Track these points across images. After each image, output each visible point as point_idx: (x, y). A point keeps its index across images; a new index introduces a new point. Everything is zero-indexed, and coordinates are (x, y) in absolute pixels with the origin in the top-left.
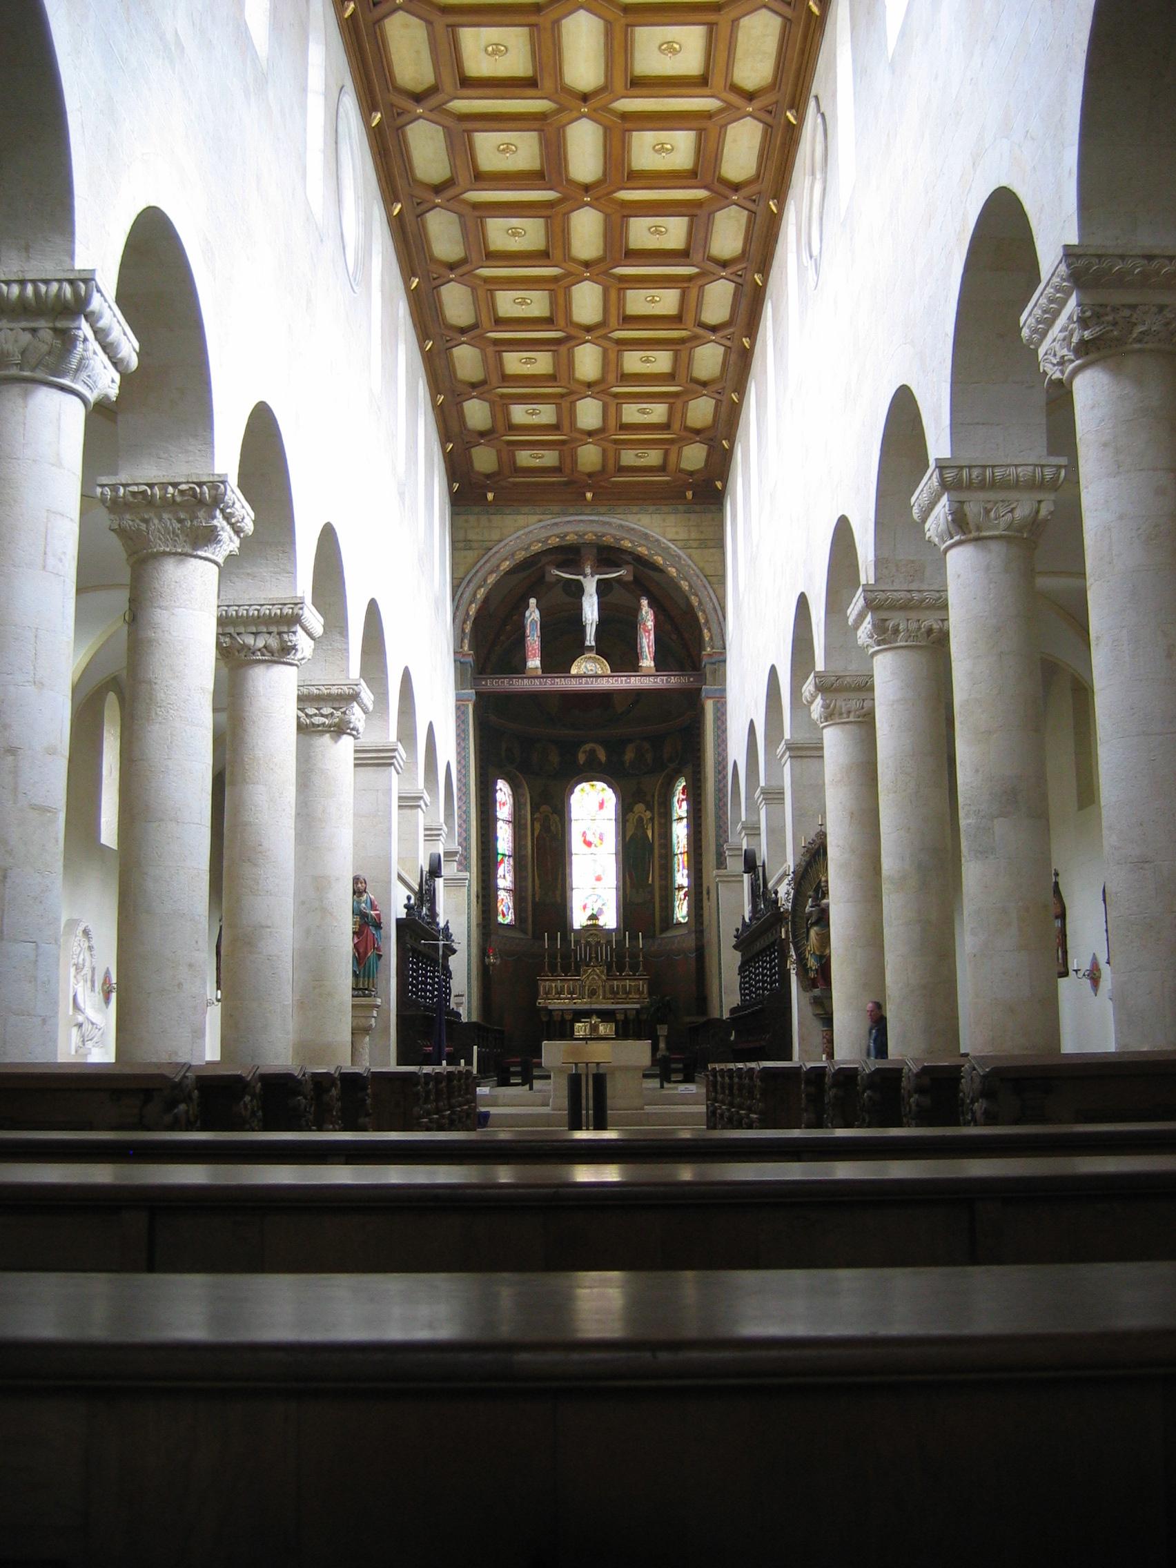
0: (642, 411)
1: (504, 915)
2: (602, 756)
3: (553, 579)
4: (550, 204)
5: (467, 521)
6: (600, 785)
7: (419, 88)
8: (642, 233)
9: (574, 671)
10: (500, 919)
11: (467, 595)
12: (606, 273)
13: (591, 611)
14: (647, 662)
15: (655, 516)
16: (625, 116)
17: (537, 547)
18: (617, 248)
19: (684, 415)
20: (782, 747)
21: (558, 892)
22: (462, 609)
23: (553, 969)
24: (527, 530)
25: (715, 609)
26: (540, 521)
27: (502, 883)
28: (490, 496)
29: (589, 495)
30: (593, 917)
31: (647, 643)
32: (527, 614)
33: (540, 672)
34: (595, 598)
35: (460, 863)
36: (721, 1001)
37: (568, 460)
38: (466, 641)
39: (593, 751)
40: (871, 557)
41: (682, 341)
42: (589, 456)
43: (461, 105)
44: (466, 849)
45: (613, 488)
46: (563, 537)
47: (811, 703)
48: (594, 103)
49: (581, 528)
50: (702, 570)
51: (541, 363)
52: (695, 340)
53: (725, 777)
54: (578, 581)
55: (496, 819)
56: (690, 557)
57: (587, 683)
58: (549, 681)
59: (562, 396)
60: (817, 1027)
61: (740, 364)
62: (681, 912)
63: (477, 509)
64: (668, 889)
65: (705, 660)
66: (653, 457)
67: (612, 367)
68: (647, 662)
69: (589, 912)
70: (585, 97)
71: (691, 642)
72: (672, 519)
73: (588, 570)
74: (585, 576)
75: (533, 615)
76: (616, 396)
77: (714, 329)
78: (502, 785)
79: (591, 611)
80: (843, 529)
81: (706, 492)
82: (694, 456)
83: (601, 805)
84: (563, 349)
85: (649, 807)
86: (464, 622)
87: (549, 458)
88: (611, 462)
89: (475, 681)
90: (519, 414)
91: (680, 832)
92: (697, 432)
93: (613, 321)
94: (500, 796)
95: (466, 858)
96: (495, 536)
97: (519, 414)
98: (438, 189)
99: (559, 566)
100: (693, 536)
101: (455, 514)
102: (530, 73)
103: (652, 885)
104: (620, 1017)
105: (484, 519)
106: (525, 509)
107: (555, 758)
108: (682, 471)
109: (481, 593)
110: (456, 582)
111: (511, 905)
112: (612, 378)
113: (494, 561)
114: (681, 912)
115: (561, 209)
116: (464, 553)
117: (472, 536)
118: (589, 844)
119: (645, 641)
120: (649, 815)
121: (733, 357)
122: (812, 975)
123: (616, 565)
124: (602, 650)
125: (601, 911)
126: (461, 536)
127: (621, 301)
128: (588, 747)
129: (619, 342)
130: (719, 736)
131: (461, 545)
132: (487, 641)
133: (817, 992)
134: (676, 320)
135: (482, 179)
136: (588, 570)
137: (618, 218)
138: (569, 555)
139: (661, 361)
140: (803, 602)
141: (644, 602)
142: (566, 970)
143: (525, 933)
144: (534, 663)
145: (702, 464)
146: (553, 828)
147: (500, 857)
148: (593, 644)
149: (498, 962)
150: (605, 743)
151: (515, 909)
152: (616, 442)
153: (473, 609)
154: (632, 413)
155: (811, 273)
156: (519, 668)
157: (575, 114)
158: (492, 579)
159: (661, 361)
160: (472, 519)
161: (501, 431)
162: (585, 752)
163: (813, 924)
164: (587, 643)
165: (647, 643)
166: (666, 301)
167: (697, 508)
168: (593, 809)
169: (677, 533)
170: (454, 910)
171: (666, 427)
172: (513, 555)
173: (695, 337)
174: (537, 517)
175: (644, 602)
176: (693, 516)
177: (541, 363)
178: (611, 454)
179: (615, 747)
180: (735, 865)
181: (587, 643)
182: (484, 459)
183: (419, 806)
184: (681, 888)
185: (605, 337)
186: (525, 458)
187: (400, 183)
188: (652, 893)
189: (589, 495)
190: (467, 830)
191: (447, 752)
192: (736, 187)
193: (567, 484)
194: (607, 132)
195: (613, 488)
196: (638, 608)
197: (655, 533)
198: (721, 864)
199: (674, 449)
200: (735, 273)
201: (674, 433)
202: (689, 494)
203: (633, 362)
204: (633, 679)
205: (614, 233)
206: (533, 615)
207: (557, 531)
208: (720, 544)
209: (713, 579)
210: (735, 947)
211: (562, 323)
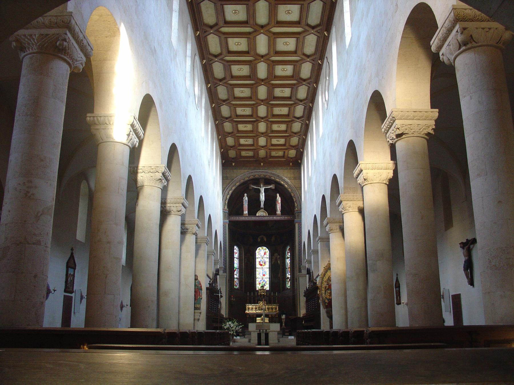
0: (278, 141)
2: (265, 240)
4: (252, 84)
6: (264, 248)
7: (216, 54)
8: (278, 92)
9: (257, 215)
11: (227, 192)
12: (268, 103)
13: (262, 197)
14: (279, 212)
16: (273, 61)
17: (247, 179)
18: (271, 97)
19: (289, 143)
20: (317, 239)
27: (235, 276)
28: (233, 164)
29: (262, 164)
30: (262, 287)
31: (279, 207)
34: (264, 194)
35: (224, 271)
39: (262, 238)
40: (343, 186)
41: (289, 121)
42: (262, 153)
43: (228, 58)
45: (270, 162)
47: (326, 226)
48: (265, 58)
49: (260, 174)
51: (249, 127)
52: (292, 121)
53: (301, 246)
55: (234, 258)
59: (254, 136)
60: (328, 320)
61: (306, 129)
62: (288, 285)
64: (284, 278)
65: (296, 212)
66: (280, 153)
67: (269, 128)
68: (279, 212)
69: (261, 285)
70: (262, 56)
71: (292, 206)
72: (286, 171)
73: (262, 186)
75: (246, 198)
76: (270, 136)
77: (298, 118)
78: (235, 247)
79: (262, 197)
80: (335, 177)
81: (296, 163)
82: (292, 153)
83: (265, 254)
84: (255, 124)
85: (279, 255)
87: (251, 154)
88: (268, 154)
89: (229, 218)
90: (242, 141)
91: (288, 261)
92: (293, 147)
93: (269, 116)
94: (235, 251)
96: (235, 176)
97: (242, 141)
98: (221, 80)
99: (253, 184)
100: (292, 176)
102: (247, 50)
108: (289, 157)
109: (231, 192)
112: (269, 132)
114: (288, 285)
115: (256, 85)
117: (228, 175)
118: (261, 265)
119: (278, 206)
120: (279, 257)
121: (303, 126)
122: (326, 304)
123: (270, 184)
124: (266, 209)
125: (264, 285)
127: (272, 111)
128: (261, 237)
129: (271, 122)
132: (233, 205)
134: (288, 116)
135: (233, 77)
137: (271, 88)
138: (256, 181)
139: (283, 127)
140: (324, 197)
141: (278, 195)
144: (246, 212)
145: (295, 156)
152: (270, 149)
153: (228, 197)
154: (274, 141)
155: (326, 105)
156: (241, 214)
157: (260, 61)
158: (234, 188)
159: (283, 127)
160: (229, 170)
161: (237, 146)
165: (279, 207)
166: (284, 111)
168: (262, 254)
170: (222, 285)
171: (284, 145)
173: (293, 120)
175: (278, 195)
176: (292, 170)
177: (249, 127)
178: (268, 153)
180: (304, 272)
182: (232, 154)
184: (288, 278)
185: (267, 120)
186: (244, 153)
187: (210, 79)
189: (262, 164)
190: (226, 261)
191: (220, 238)
192: (304, 80)
193: (255, 161)
194: (269, 65)
195: (270, 162)
196: (276, 197)
197: (281, 175)
198: (300, 271)
199: (286, 152)
200: (304, 103)
201: (287, 146)
202: (291, 164)
203: (275, 127)
205: (270, 93)
206: (246, 198)
207: (253, 174)
209: (298, 189)
210: (304, 296)
211: (255, 116)
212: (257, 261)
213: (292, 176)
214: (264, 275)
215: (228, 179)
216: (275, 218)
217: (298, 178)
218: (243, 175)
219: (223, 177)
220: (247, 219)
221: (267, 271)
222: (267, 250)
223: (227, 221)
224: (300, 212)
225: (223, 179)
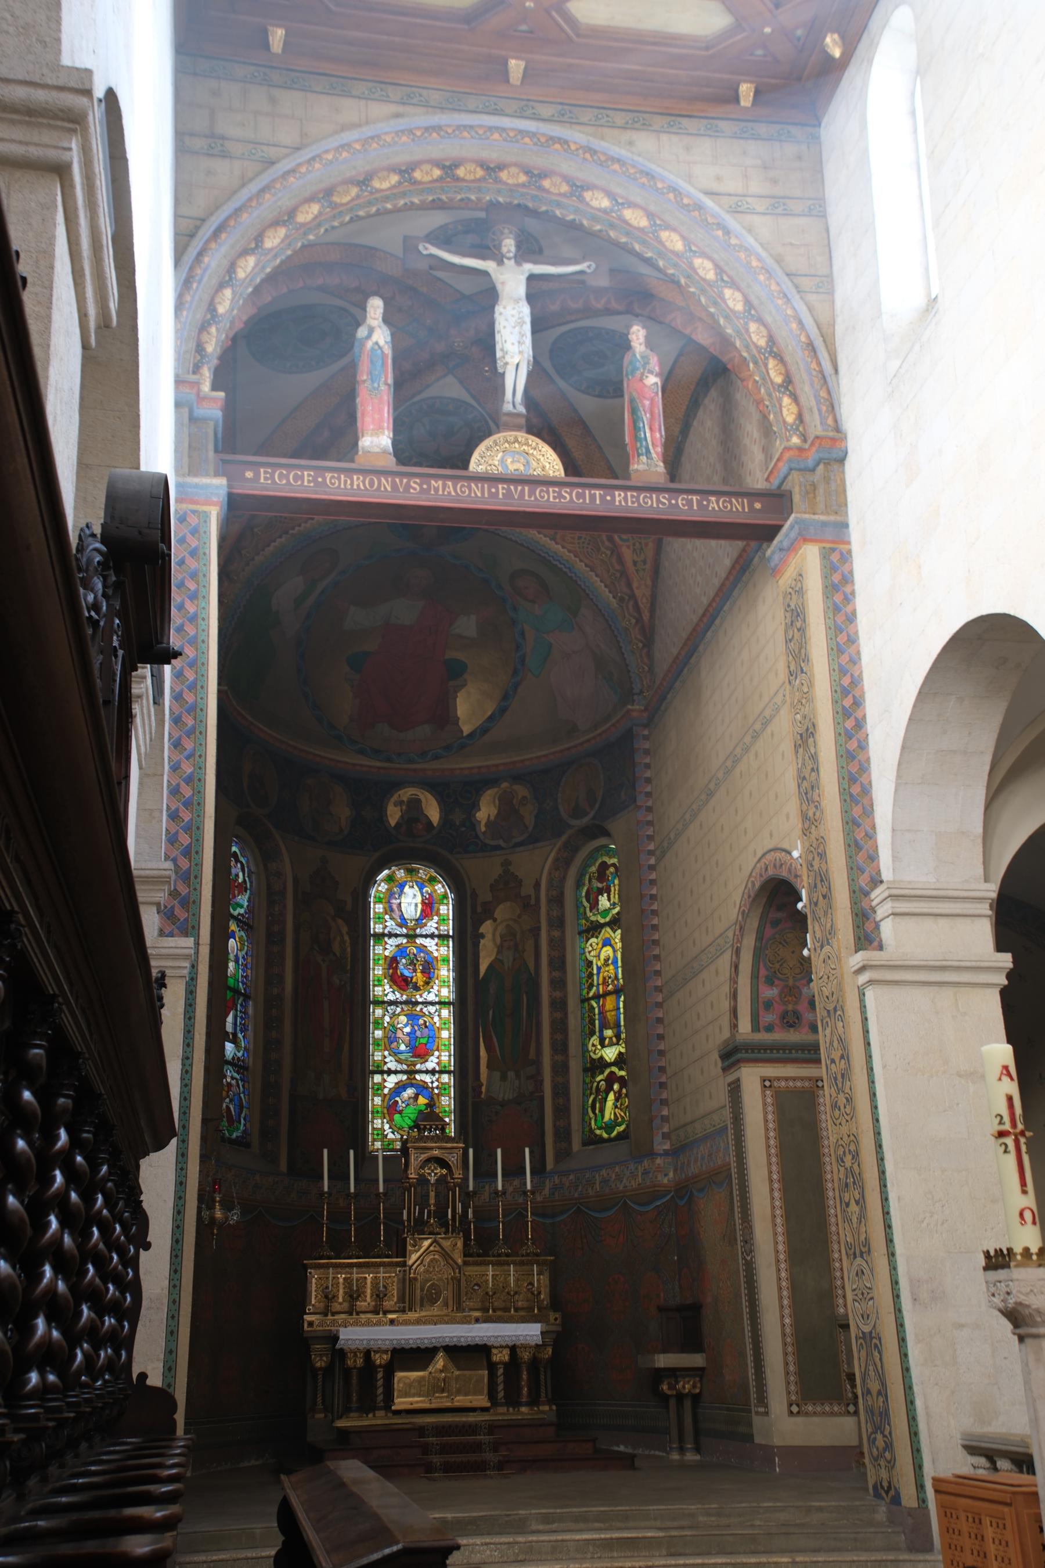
2: (433, 812)
9: (477, 464)
15: (664, 137)
22: (200, 292)
23: (339, 1247)
24: (367, 131)
25: (811, 347)
26: (398, 115)
28: (277, 36)
32: (362, 332)
33: (390, 462)
36: (900, 1325)
38: (207, 375)
39: (415, 804)
44: (189, 877)
46: (449, 168)
50: (779, 260)
54: (486, 274)
56: (750, 231)
57: (508, 494)
58: (415, 485)
72: (705, 146)
83: (429, 907)
86: (203, 328)
95: (189, 903)
103: (538, 1063)
104: (501, 1356)
107: (343, 812)
113: (286, 202)
128: (407, 793)
130: (838, 630)
136: (509, 245)
142: (367, 1247)
144: (377, 440)
147: (229, 994)
148: (522, 409)
149: (235, 1217)
150: (439, 788)
162: (400, 803)
164: (508, 407)
167: (763, 129)
169: (718, 179)
172: (329, 192)
174: (393, 108)
179: (458, 795)
181: (508, 407)
183: (61, 171)
188: (537, 1079)
189: (516, 66)
198: (866, 937)
204: (619, 496)
208: (817, 209)
209: (805, 283)
212: (380, 952)
213: (756, 186)
214: (421, 1052)
215: (225, 155)
216: (622, 502)
217: (806, 200)
221: (443, 1023)
222: (440, 888)
223: (217, 486)
224: (830, 453)
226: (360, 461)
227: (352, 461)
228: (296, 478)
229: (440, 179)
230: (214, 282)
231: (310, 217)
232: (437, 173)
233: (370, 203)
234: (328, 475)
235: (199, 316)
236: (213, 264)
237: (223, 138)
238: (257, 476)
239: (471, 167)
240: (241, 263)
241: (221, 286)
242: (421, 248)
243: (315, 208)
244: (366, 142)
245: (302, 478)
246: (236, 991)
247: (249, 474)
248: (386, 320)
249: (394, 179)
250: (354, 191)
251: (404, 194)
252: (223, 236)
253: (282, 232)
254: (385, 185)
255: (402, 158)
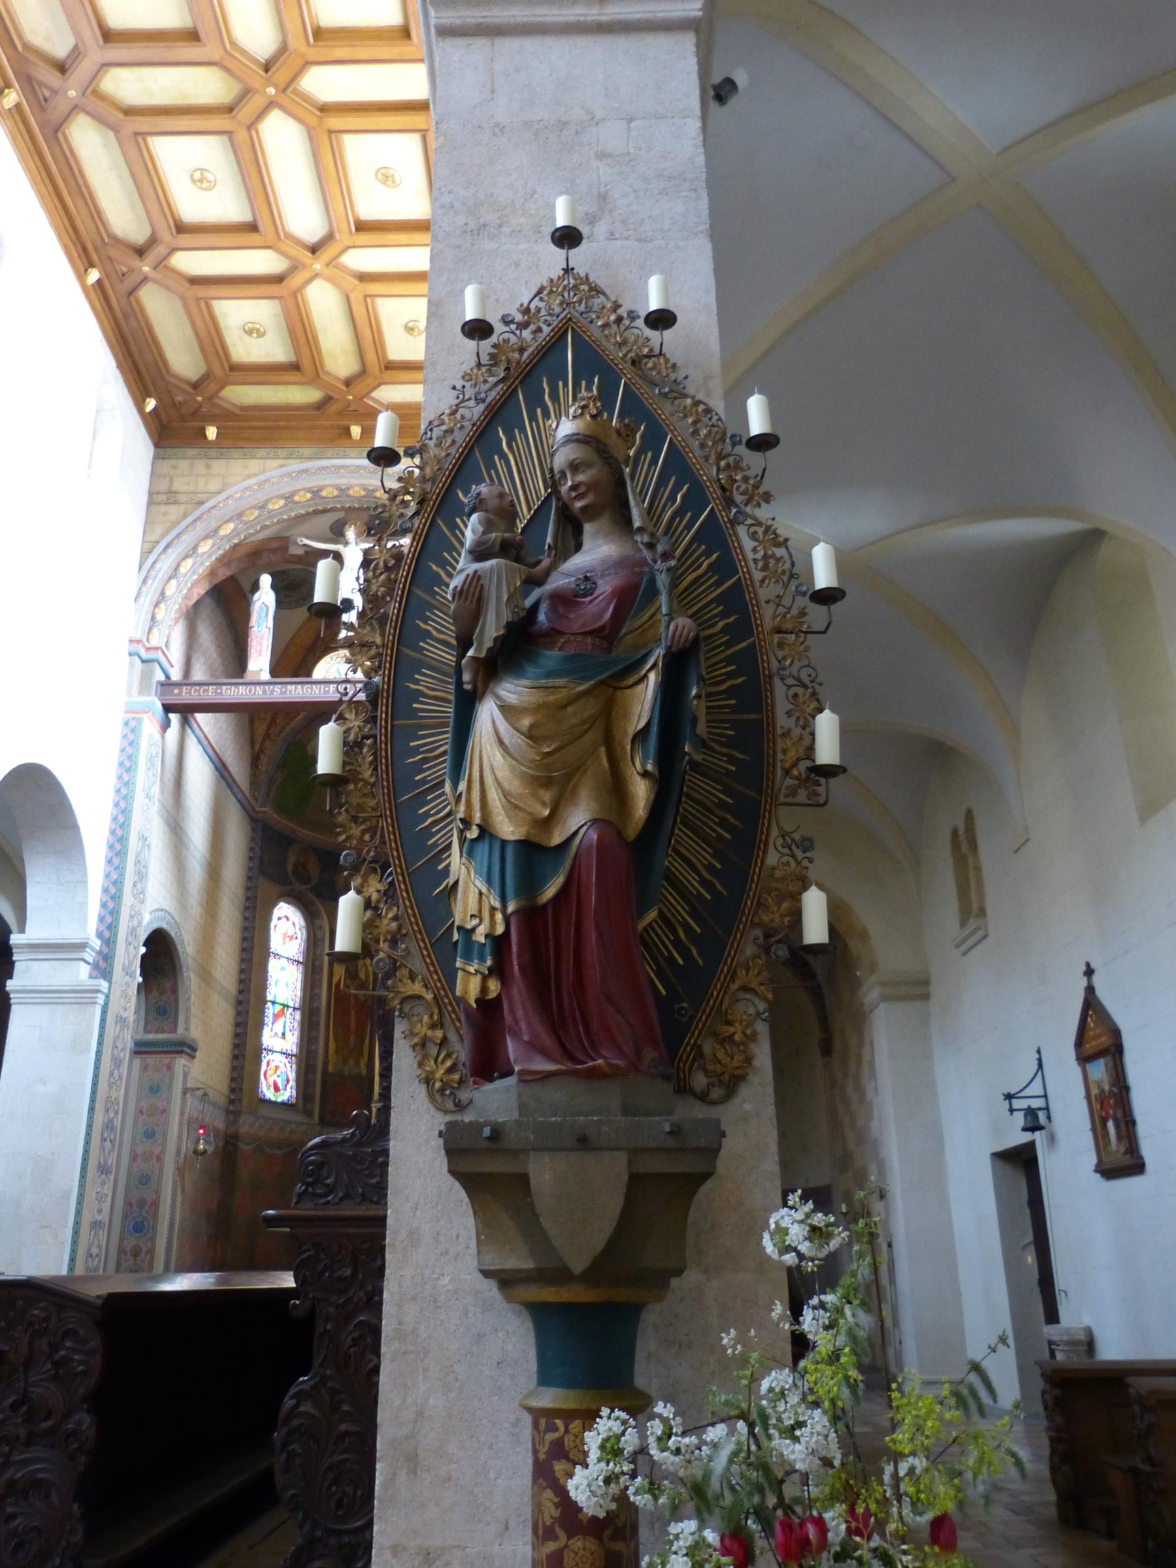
1: (277, 1089)
3: (300, 552)
5: (174, 467)
10: (269, 1094)
11: (165, 565)
21: (364, 1062)
26: (283, 466)
33: (266, 676)
35: (96, 966)
37: (305, 351)
46: (316, 492)
49: (343, 481)
58: (277, 688)
63: (190, 452)
73: (351, 534)
74: (346, 543)
96: (214, 486)
101: (156, 458)
105: (200, 466)
106: (262, 452)
110: (147, 545)
111: (292, 1076)
113: (213, 524)
116: (163, 508)
117: (178, 485)
122: (471, 982)
126: (163, 486)
131: (162, 498)
133: (495, 1101)
143: (310, 1114)
146: (362, 975)
151: (298, 1080)
160: (184, 464)
163: (493, 667)
172: (241, 515)
174: (280, 462)
193: (320, 406)
215: (175, 503)
218: (255, 488)
219: (151, 494)
220: (258, 695)
225: (151, 503)
226: (249, 677)
227: (242, 677)
228: (205, 691)
229: (311, 499)
230: (166, 577)
231: (228, 532)
232: (309, 496)
233: (270, 517)
234: (224, 688)
235: (155, 599)
236: (165, 567)
237: (176, 493)
238: (180, 694)
239: (330, 489)
240: (183, 564)
241: (170, 578)
242: (299, 540)
243: (231, 526)
244: (260, 484)
245: (207, 691)
246: (286, 1006)
247: (176, 691)
248: (273, 587)
249: (282, 502)
250: (256, 513)
251: (292, 510)
252: (170, 550)
253: (210, 542)
254: (277, 507)
255: (286, 490)
